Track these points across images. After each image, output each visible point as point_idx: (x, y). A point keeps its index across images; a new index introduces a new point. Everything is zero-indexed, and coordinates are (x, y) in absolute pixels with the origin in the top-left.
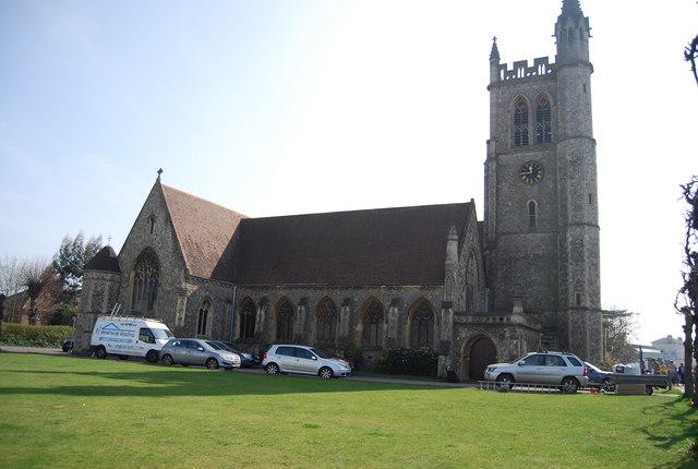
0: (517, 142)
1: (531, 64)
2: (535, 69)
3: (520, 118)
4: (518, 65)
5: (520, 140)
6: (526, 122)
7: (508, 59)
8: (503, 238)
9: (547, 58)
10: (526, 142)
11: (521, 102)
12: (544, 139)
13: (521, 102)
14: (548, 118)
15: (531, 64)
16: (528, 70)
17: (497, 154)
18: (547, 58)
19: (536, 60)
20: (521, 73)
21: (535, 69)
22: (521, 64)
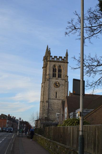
0: (53, 76)
1: (58, 58)
2: (59, 59)
3: (54, 70)
4: (55, 57)
5: (54, 75)
6: (56, 71)
7: (53, 54)
8: (49, 100)
9: (62, 57)
10: (55, 77)
11: (55, 66)
12: (60, 76)
13: (55, 66)
14: (61, 72)
15: (58, 58)
16: (57, 59)
17: (49, 79)
18: (60, 57)
19: (60, 57)
20: (55, 59)
21: (59, 59)
22: (55, 57)
